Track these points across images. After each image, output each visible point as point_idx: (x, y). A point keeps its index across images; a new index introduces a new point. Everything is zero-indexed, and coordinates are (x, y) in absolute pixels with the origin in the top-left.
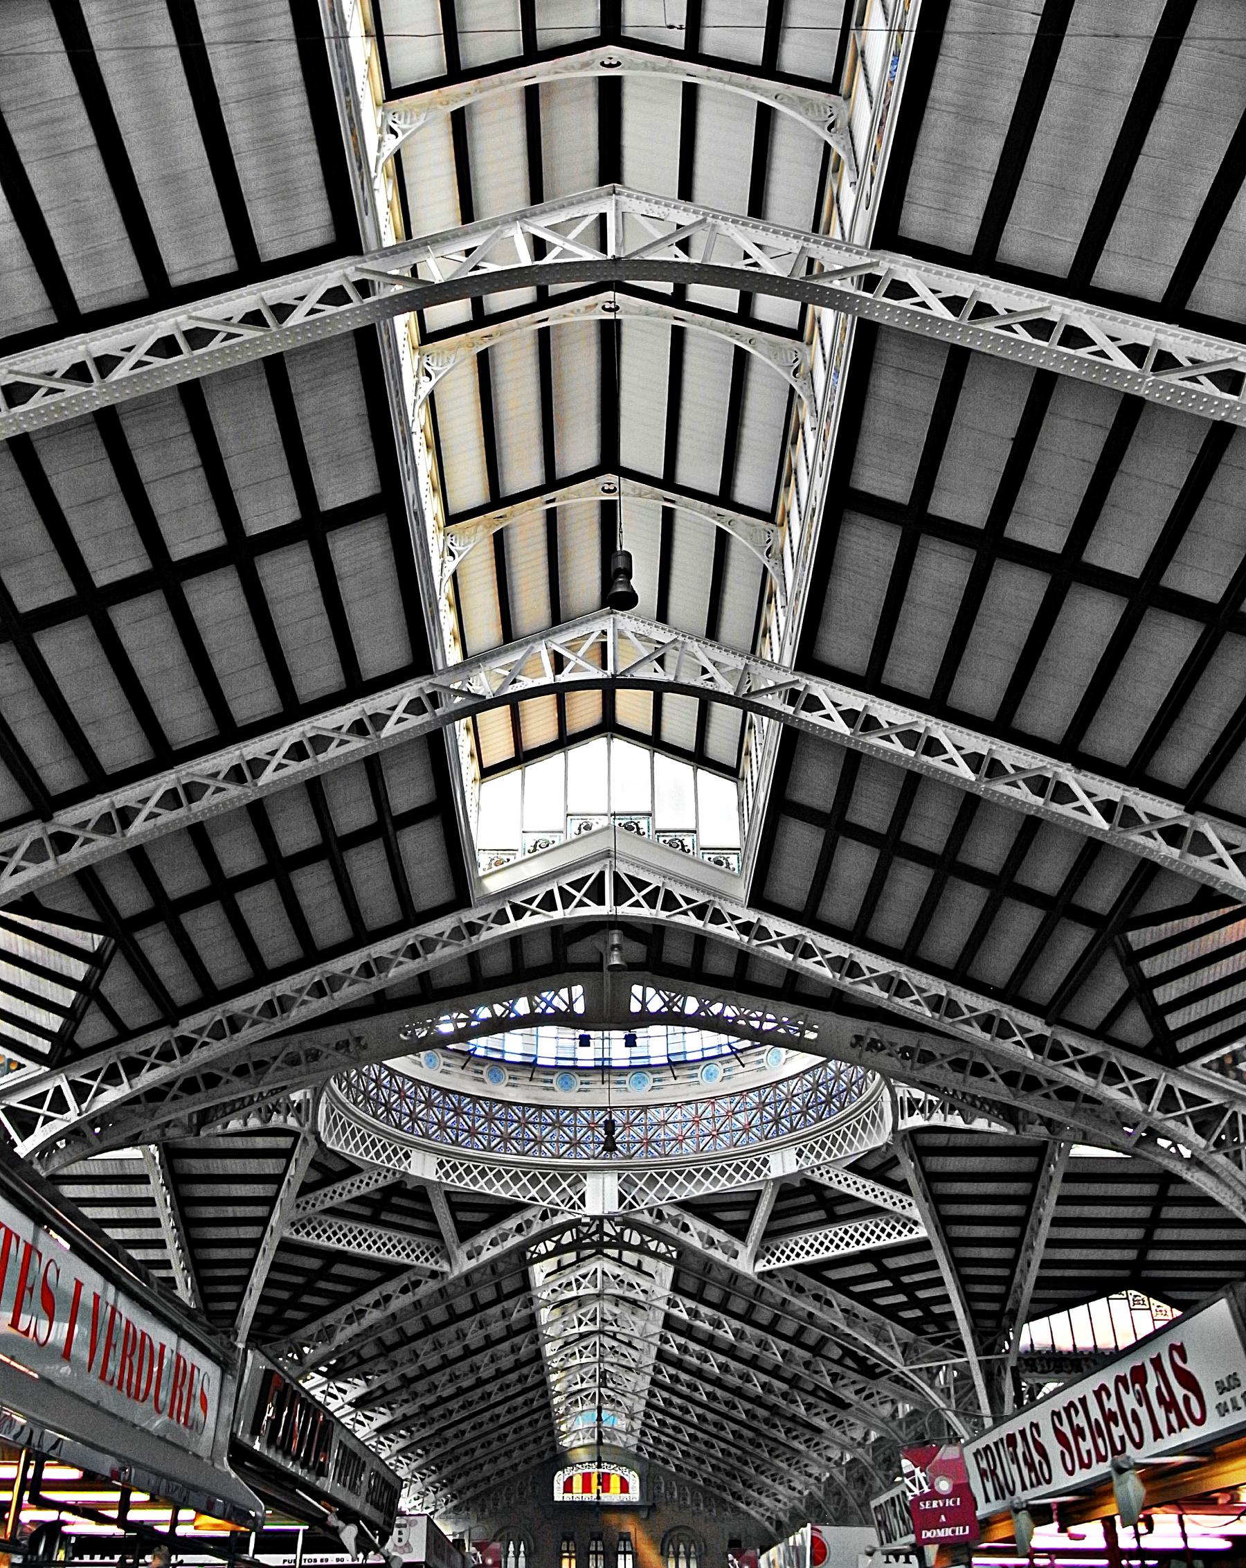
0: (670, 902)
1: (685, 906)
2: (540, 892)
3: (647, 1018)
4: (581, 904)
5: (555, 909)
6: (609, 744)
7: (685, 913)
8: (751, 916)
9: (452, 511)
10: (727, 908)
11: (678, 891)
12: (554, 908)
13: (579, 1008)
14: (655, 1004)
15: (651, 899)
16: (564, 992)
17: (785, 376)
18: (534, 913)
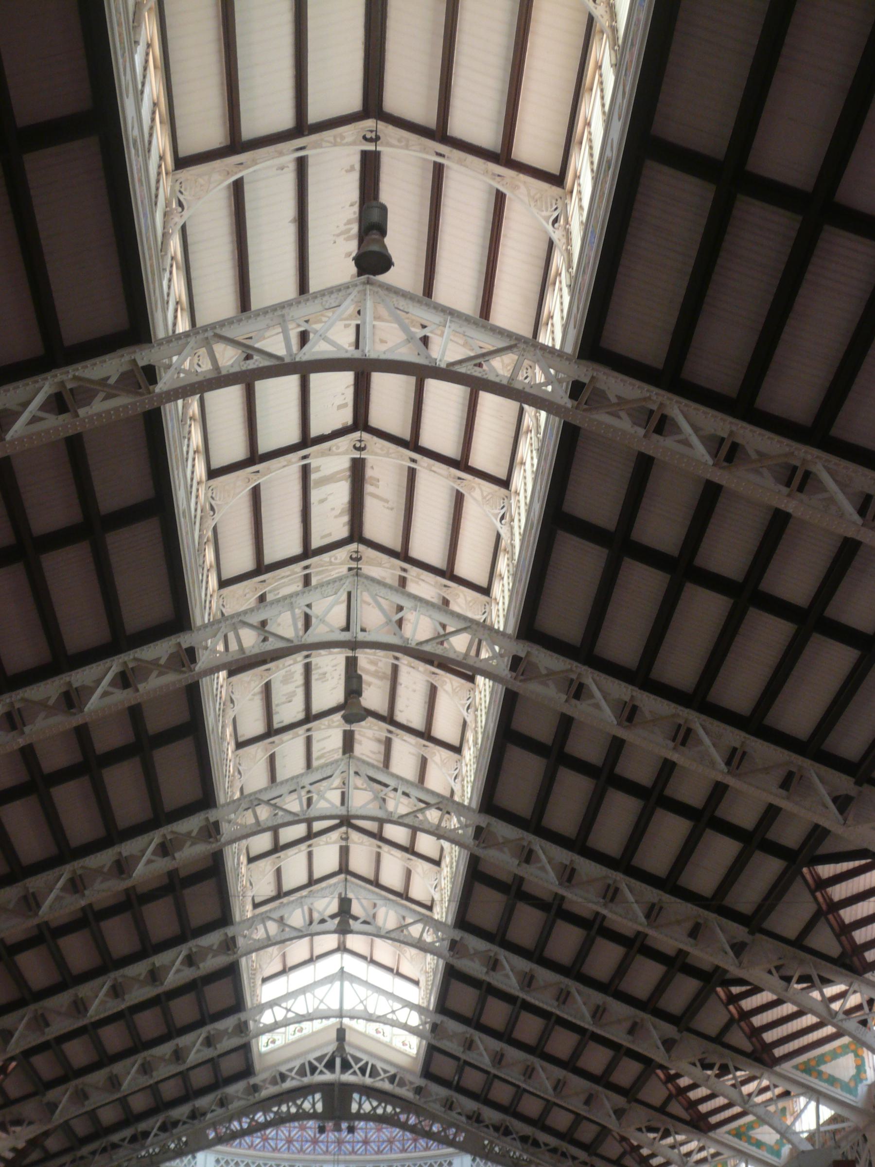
0: (374, 1073)
1: (383, 1075)
2: (297, 1064)
3: (359, 1116)
4: (321, 1072)
5: (306, 1075)
6: (342, 958)
7: (383, 1080)
8: (422, 1082)
9: (240, 740)
10: (409, 1077)
11: (379, 1065)
12: (306, 1075)
13: (319, 1107)
14: (367, 1107)
15: (363, 1070)
16: (310, 1098)
17: (430, 888)
18: (293, 1078)
